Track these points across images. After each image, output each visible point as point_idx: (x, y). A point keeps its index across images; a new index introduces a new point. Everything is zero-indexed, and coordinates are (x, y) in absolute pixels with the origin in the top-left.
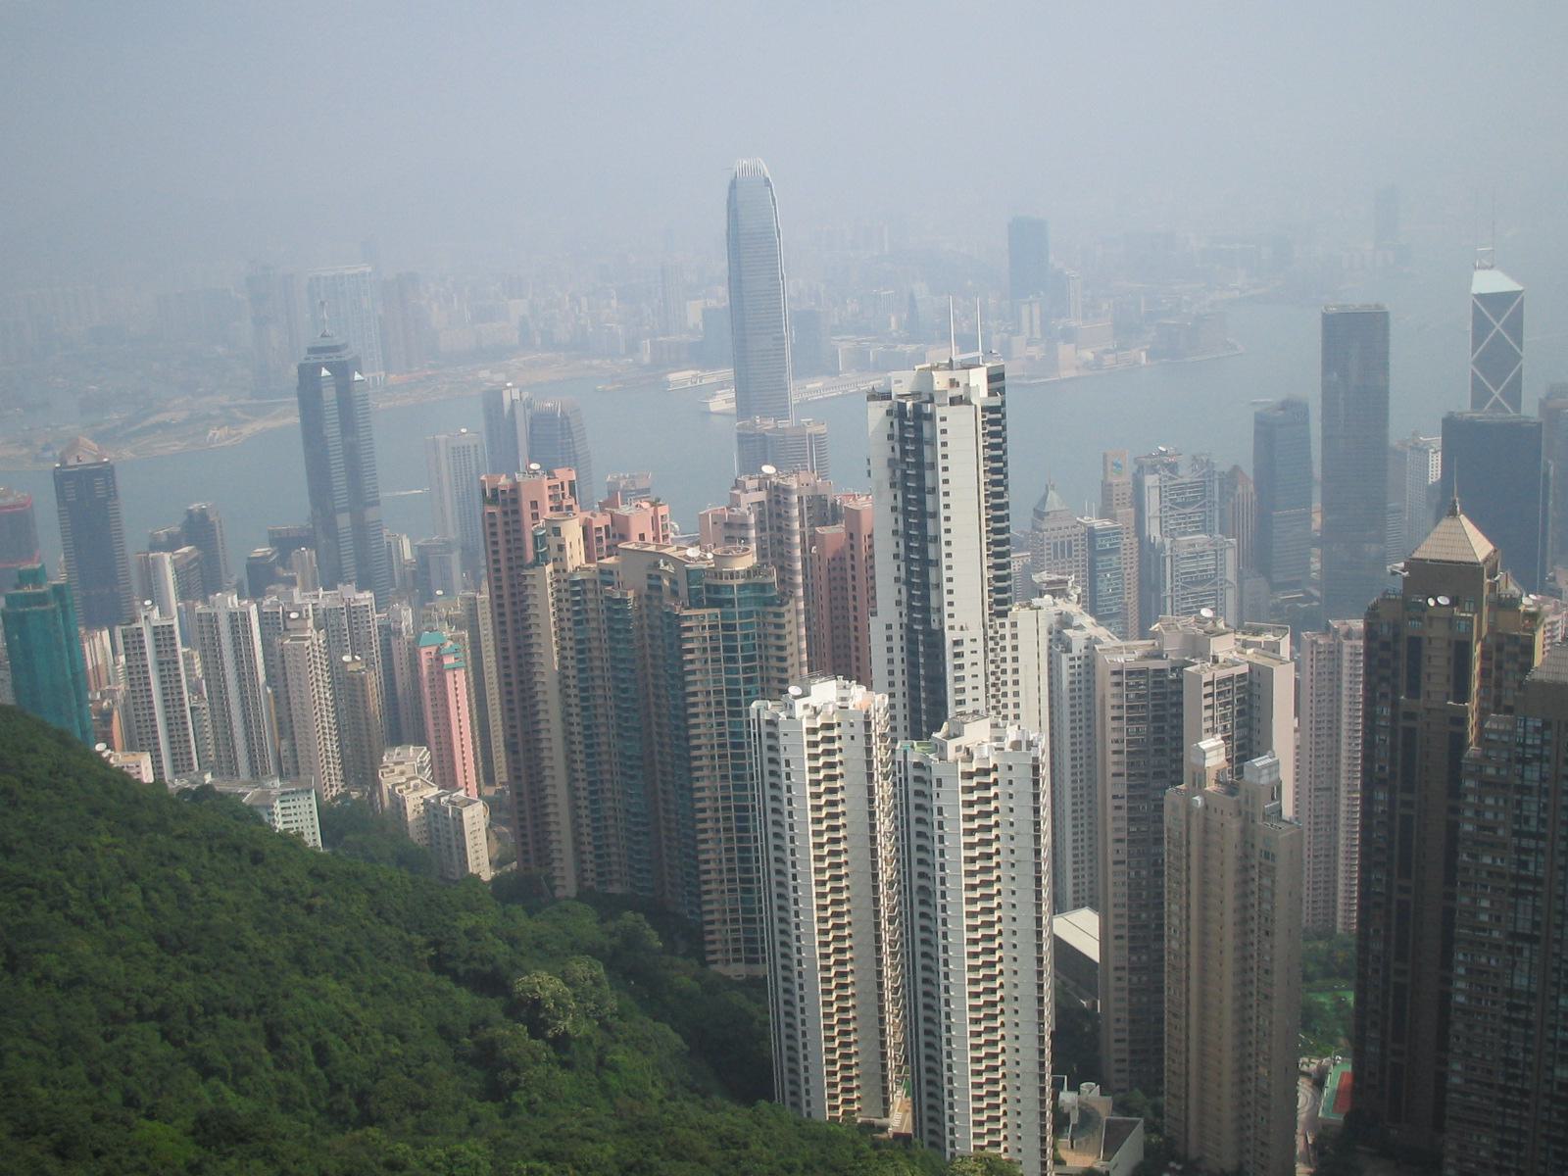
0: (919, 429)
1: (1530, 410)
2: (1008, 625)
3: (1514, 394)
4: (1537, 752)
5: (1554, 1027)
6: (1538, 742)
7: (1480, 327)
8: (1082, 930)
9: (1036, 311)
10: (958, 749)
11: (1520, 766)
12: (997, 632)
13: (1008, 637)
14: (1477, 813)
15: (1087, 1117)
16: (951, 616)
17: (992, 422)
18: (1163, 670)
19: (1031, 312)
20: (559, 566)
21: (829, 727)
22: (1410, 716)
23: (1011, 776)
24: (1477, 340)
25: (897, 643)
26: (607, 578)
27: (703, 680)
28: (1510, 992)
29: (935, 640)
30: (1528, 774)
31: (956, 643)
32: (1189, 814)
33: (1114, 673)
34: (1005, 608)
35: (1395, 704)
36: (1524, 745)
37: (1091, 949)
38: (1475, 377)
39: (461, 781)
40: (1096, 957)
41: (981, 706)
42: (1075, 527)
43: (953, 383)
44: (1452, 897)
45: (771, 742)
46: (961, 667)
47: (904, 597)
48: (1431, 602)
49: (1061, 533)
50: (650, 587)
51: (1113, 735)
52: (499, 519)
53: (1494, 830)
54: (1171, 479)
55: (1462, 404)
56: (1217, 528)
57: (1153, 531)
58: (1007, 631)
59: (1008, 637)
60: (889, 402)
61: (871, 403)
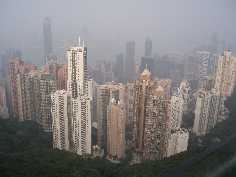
0: (75, 55)
1: (152, 57)
3: (150, 54)
5: (157, 135)
8: (96, 125)
10: (80, 99)
15: (97, 149)
16: (78, 81)
17: (85, 55)
20: (21, 73)
21: (62, 96)
22: (140, 95)
23: (87, 103)
24: (146, 48)
25: (71, 85)
26: (28, 75)
27: (43, 90)
28: (152, 131)
29: (76, 85)
31: (80, 85)
32: (111, 109)
35: (138, 94)
37: (96, 127)
39: (4, 105)
40: (97, 128)
41: (82, 94)
43: (80, 49)
44: (145, 119)
45: (54, 98)
46: (80, 88)
47: (72, 79)
50: (35, 77)
51: (100, 98)
52: (12, 66)
53: (150, 110)
55: (144, 55)
57: (102, 70)
58: (86, 84)
61: (68, 52)
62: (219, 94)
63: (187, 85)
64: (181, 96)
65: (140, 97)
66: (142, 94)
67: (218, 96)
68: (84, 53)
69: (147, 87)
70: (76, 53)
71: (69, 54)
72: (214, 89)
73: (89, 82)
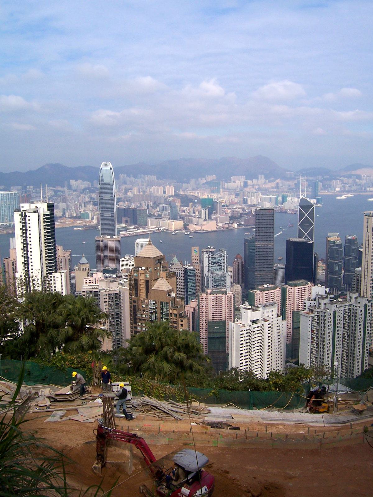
0: (25, 219)
2: (53, 277)
3: (311, 235)
4: (154, 310)
6: (154, 308)
7: (301, 215)
9: (207, 211)
11: (150, 315)
12: (49, 279)
13: (53, 280)
14: (141, 328)
18: (97, 292)
19: (206, 211)
22: (135, 302)
30: (152, 317)
33: (83, 292)
34: (52, 272)
36: (151, 308)
38: (300, 230)
42: (181, 268)
43: (36, 207)
48: (140, 269)
49: (179, 270)
54: (212, 255)
56: (225, 271)
57: (206, 269)
58: (52, 278)
59: (53, 280)
60: (20, 213)
61: (15, 212)
62: (362, 308)
63: (326, 292)
64: (272, 311)
65: (135, 306)
66: (141, 299)
67: (358, 311)
68: (44, 215)
69: (147, 282)
70: (28, 214)
71: (17, 217)
72: (351, 295)
73: (57, 275)
